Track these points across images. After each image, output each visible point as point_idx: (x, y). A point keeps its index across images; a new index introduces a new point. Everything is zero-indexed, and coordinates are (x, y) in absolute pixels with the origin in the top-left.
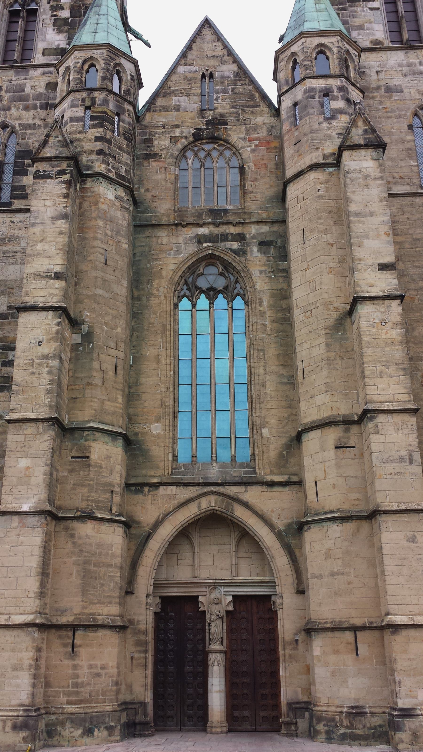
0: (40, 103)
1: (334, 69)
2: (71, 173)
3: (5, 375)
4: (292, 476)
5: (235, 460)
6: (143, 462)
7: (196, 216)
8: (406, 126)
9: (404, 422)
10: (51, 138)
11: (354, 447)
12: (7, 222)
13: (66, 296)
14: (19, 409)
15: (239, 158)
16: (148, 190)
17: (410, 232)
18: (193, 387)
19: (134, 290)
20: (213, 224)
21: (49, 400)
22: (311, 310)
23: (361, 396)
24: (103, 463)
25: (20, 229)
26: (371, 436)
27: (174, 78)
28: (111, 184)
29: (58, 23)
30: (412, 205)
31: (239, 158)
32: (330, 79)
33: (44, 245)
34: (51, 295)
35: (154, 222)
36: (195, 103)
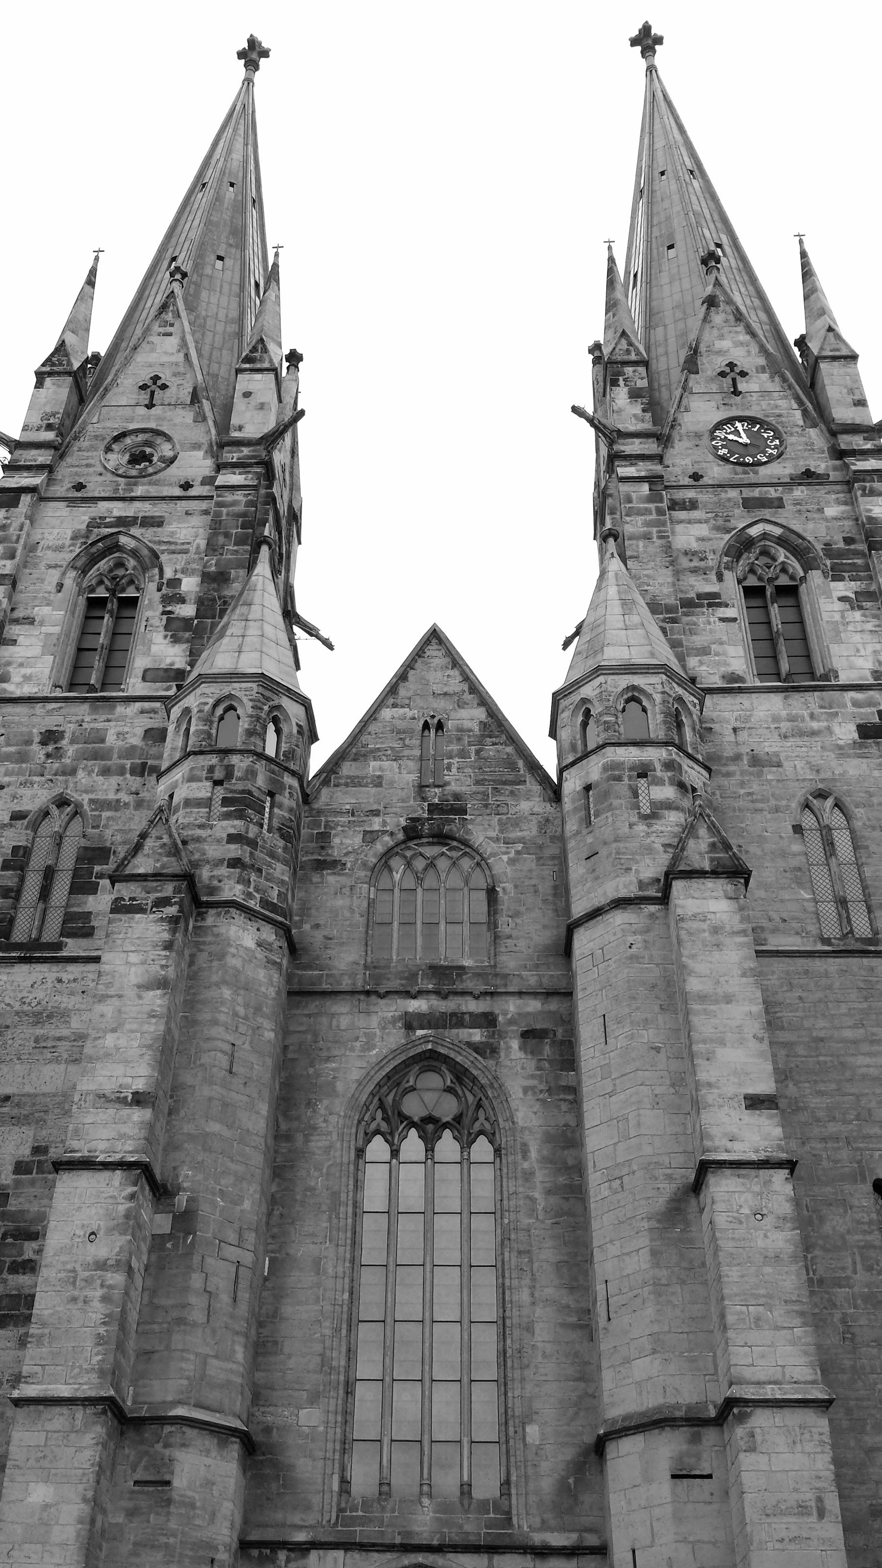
0: (132, 764)
1: (655, 731)
2: (180, 904)
3: (14, 1292)
4: (585, 1535)
5: (470, 1493)
6: (278, 1494)
7: (406, 979)
8: (790, 827)
9: (805, 1428)
10: (148, 840)
11: (709, 1476)
12: (49, 981)
13: (150, 1140)
14: (40, 1375)
15: (487, 872)
16: (317, 926)
17: (807, 1024)
18: (388, 1328)
19: (281, 1119)
20: (437, 992)
21: (100, 1357)
22: (621, 1178)
23: (722, 1365)
24: (197, 1497)
25: (72, 994)
26: (742, 1456)
27: (373, 728)
29: (174, 625)
30: (807, 972)
31: (487, 872)
34: (122, 1136)
35: (325, 987)
36: (409, 773)
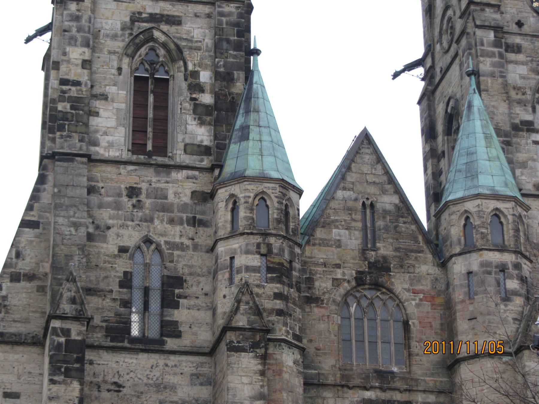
0: (187, 217)
1: (509, 240)
7: (364, 379)
10: (241, 304)
15: (403, 311)
16: (311, 341)
25: (175, 374)
28: (290, 348)
31: (403, 311)
32: (506, 254)
36: (356, 239)
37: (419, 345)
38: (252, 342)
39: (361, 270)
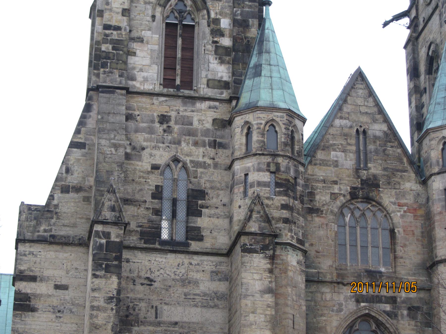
0: (209, 140)
7: (356, 277)
10: (254, 213)
15: (390, 221)
16: (312, 245)
25: (198, 271)
28: (294, 251)
31: (390, 221)
33: (255, 317)
36: (351, 160)
37: (403, 249)
38: (262, 245)
39: (355, 186)
